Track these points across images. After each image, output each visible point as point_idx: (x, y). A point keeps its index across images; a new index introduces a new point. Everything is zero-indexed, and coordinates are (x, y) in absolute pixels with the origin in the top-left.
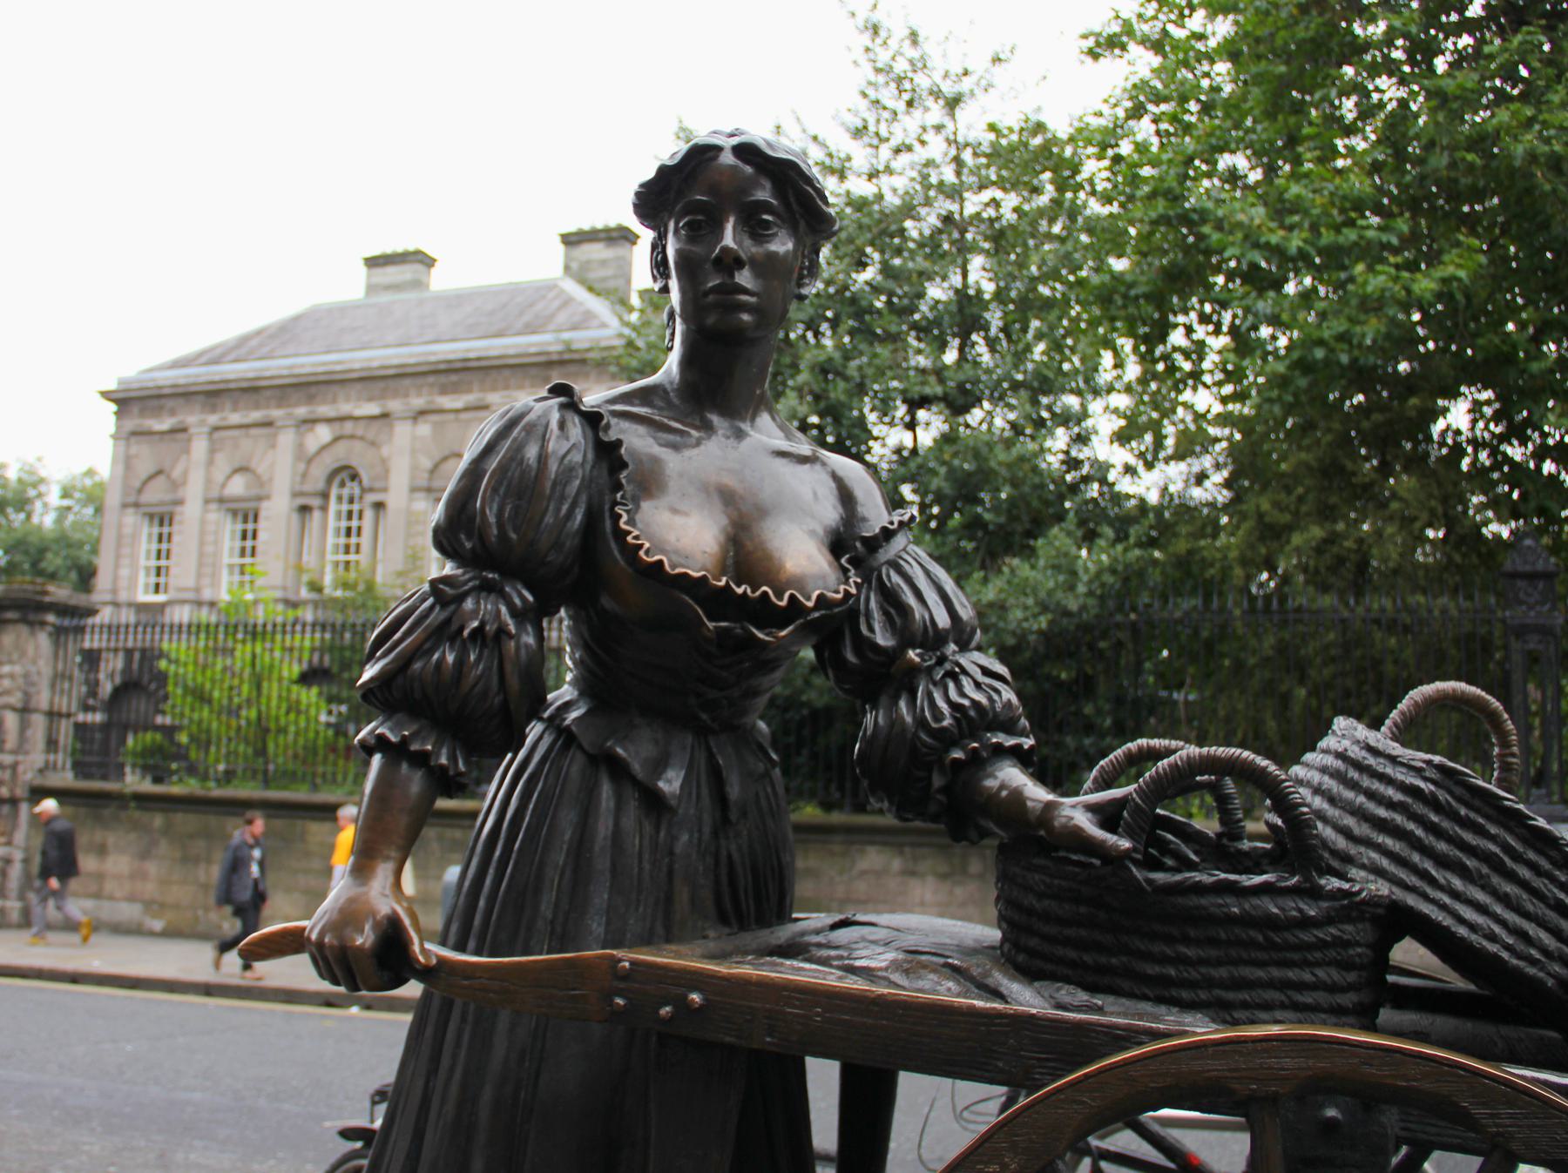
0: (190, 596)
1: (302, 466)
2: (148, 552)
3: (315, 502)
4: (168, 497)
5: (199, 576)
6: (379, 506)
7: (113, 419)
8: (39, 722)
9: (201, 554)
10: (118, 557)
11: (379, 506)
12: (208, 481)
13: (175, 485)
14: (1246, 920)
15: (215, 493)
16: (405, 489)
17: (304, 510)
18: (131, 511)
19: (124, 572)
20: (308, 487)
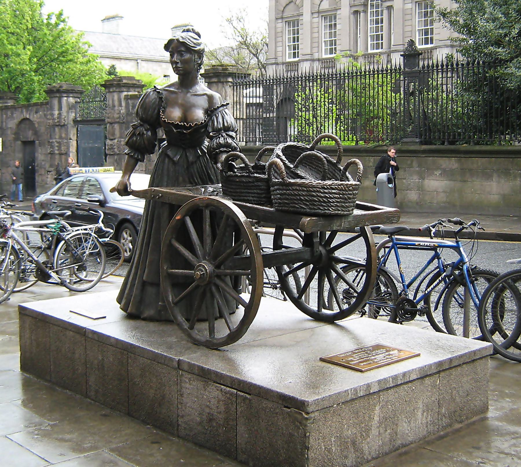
2: (289, 39)
3: (361, 9)
4: (295, 13)
5: (312, 48)
6: (390, 8)
9: (312, 38)
14: (239, 182)
15: (316, 10)
17: (356, 13)
18: (280, 21)
19: (280, 49)
20: (356, 3)
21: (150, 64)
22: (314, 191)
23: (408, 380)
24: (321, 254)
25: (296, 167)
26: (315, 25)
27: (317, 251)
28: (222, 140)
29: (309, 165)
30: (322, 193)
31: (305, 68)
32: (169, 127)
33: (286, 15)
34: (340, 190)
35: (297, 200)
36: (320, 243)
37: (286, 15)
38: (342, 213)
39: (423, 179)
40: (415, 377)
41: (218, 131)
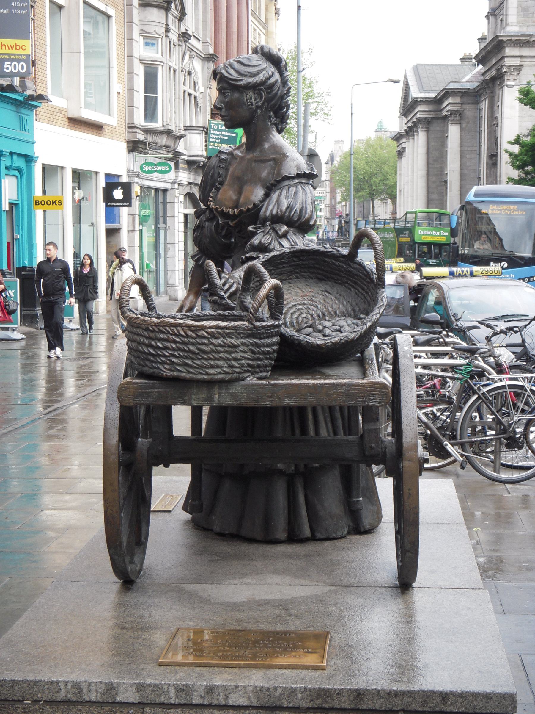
23: (223, 703)
27: (371, 448)
29: (353, 287)
30: (147, 338)
34: (175, 335)
38: (188, 376)
40: (243, 701)
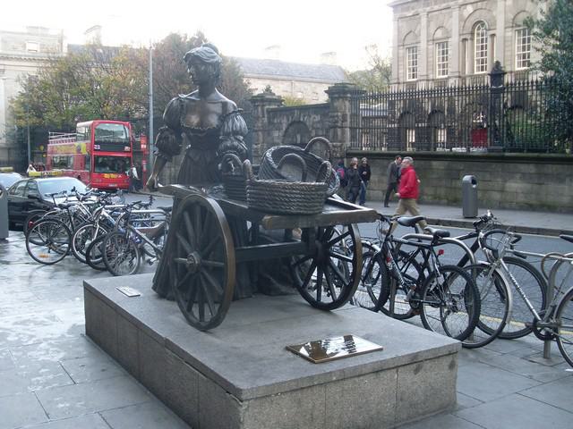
0: (425, 78)
1: (462, 24)
5: (427, 70)
7: (392, 13)
8: (348, 130)
10: (398, 65)
11: (493, 35)
12: (428, 34)
13: (417, 36)
16: (503, 28)
19: (401, 71)
21: (302, 84)
22: (276, 191)
24: (317, 249)
25: (280, 168)
26: (430, 51)
28: (229, 144)
31: (422, 86)
32: (188, 130)
33: (406, 43)
35: (262, 199)
36: (318, 239)
37: (406, 43)
39: (505, 181)
41: (228, 135)
